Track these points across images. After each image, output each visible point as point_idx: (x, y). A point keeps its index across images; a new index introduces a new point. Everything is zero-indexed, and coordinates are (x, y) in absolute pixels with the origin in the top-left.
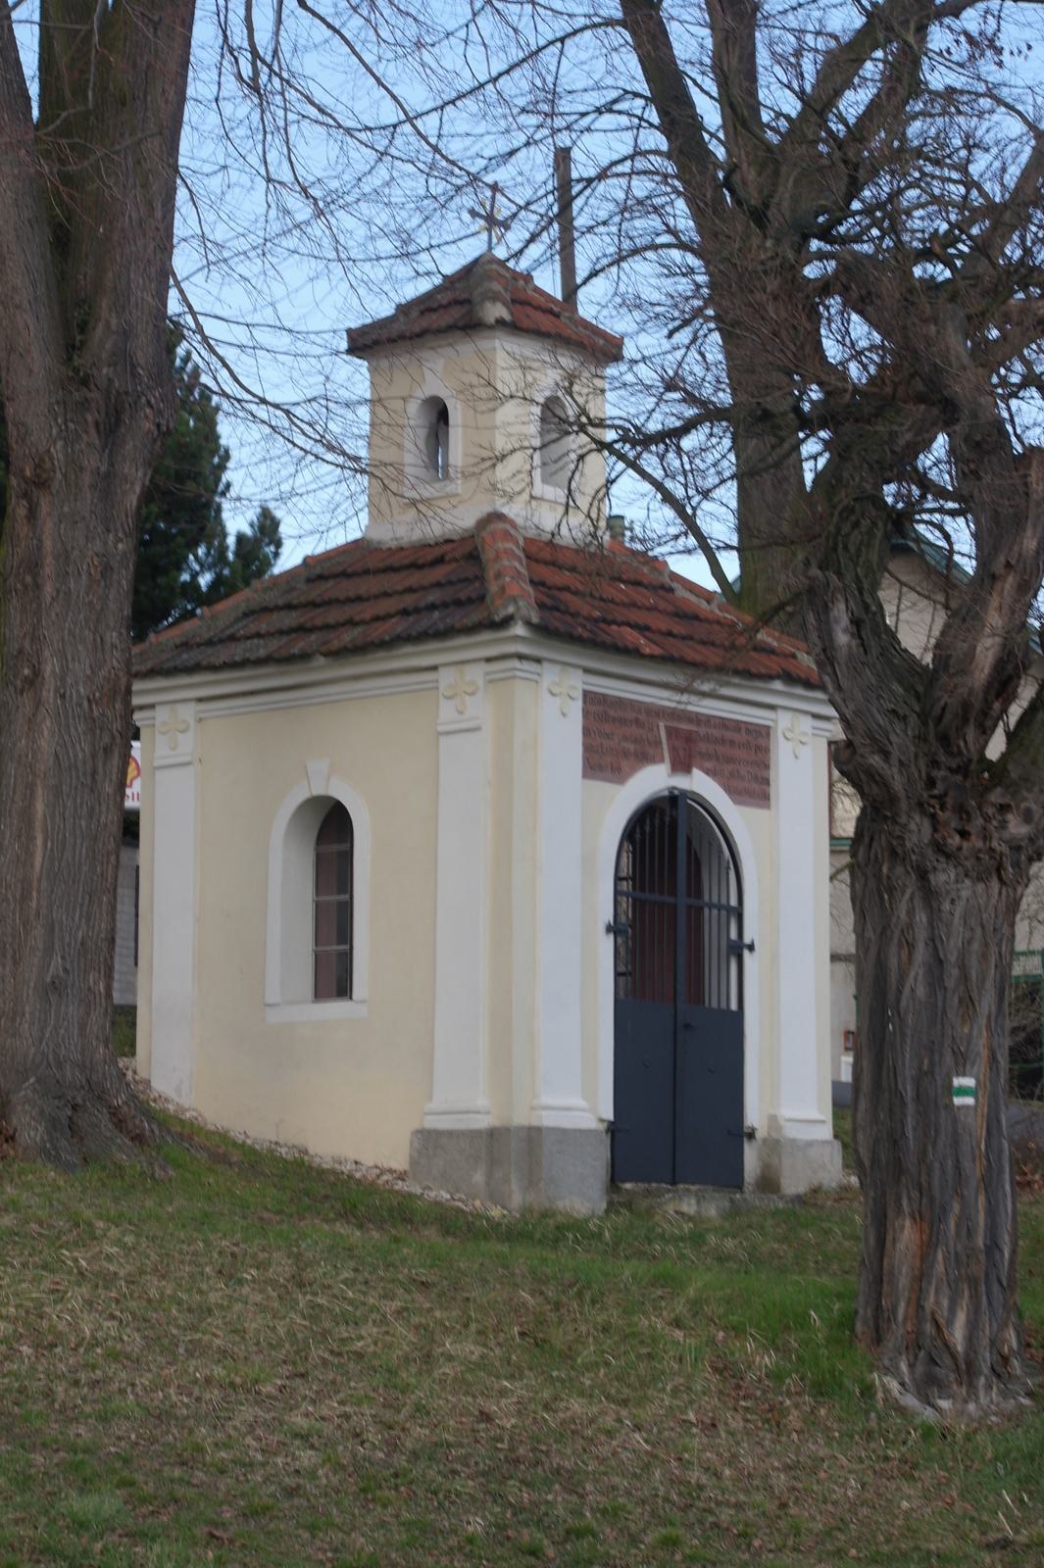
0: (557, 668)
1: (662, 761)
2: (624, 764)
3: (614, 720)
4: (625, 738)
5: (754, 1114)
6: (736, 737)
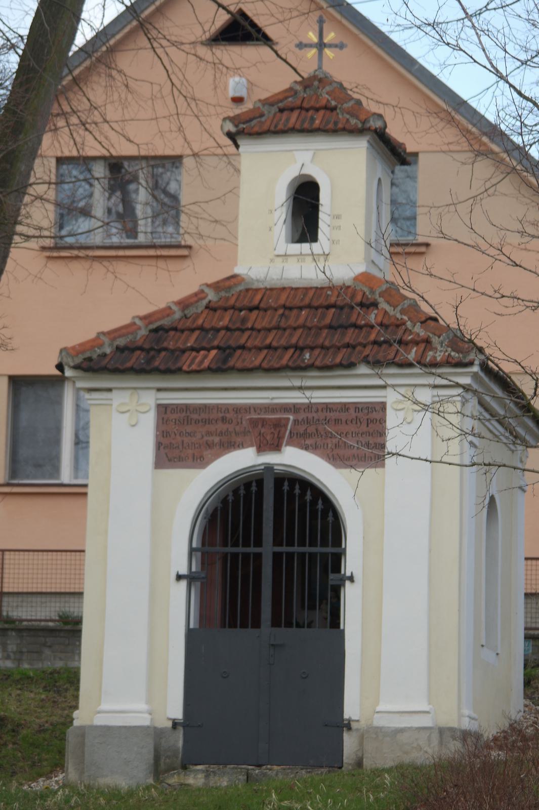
0: (129, 392)
2: (207, 453)
3: (197, 422)
4: (209, 433)
5: (351, 709)
6: (343, 416)
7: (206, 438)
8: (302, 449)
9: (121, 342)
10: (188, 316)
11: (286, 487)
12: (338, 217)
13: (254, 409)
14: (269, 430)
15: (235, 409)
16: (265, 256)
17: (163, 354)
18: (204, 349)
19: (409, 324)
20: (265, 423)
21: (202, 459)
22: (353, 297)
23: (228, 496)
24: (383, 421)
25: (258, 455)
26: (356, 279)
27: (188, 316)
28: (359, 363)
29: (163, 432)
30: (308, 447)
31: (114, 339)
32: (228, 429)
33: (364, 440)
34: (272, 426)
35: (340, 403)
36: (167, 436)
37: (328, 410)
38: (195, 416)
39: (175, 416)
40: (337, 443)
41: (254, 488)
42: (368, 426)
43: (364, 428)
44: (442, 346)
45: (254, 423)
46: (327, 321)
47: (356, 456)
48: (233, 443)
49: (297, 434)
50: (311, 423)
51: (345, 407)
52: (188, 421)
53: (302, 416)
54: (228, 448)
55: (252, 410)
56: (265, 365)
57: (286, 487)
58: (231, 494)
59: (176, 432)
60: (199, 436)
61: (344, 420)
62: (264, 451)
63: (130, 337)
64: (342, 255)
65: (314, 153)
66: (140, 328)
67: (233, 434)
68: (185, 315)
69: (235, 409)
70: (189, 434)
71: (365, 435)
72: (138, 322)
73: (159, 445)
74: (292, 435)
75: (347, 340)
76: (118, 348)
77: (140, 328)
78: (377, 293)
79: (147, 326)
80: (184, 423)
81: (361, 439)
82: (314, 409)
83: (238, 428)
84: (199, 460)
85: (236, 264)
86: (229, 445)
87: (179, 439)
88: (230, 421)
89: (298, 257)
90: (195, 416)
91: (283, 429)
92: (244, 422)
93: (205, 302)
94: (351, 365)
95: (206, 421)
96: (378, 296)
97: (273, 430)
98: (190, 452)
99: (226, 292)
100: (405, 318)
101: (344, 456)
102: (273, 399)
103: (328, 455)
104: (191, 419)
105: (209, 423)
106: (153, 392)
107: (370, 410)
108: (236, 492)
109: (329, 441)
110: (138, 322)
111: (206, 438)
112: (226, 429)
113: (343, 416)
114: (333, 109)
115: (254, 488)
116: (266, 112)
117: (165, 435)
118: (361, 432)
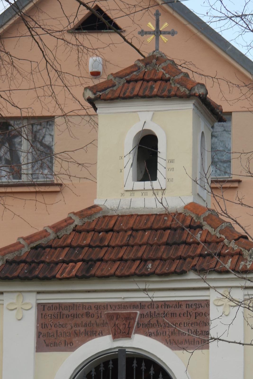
0: (16, 295)
1: (110, 334)
2: (75, 340)
3: (67, 316)
4: (77, 325)
6: (177, 311)
7: (74, 329)
8: (147, 336)
9: (10, 257)
10: (60, 237)
11: (135, 365)
12: (172, 161)
13: (110, 306)
14: (122, 322)
15: (96, 307)
16: (116, 190)
17: (42, 265)
18: (72, 261)
19: (226, 241)
20: (118, 317)
21: (71, 344)
22: (183, 221)
23: (91, 371)
24: (207, 314)
25: (114, 341)
26: (186, 207)
27: (60, 237)
28: (189, 271)
29: (42, 324)
30: (151, 334)
31: (4, 255)
32: (90, 321)
33: (192, 328)
34: (124, 319)
35: (175, 301)
36: (45, 327)
37: (166, 306)
38: (66, 312)
39: (50, 312)
40: (173, 331)
41: (111, 366)
42: (196, 318)
43: (193, 319)
44: (251, 258)
45: (110, 317)
46: (165, 239)
47: (187, 341)
48: (94, 332)
49: (143, 324)
50: (153, 316)
51: (178, 304)
52: (61, 316)
53: (146, 311)
54: (91, 336)
55: (109, 307)
56: (118, 273)
57: (135, 365)
58: (94, 370)
59: (52, 324)
60: (69, 327)
61: (178, 314)
62: (118, 337)
63: (17, 253)
64: (176, 188)
65: (154, 114)
66: (23, 247)
67: (95, 326)
68: (58, 236)
69: (96, 307)
70: (62, 326)
71: (194, 325)
72: (22, 242)
73: (39, 335)
74: (139, 325)
75: (179, 254)
76: (7, 261)
77: (23, 247)
78: (202, 218)
79: (29, 245)
80: (57, 318)
81: (191, 328)
82: (155, 305)
83: (98, 321)
84: (69, 345)
85: (96, 198)
86: (92, 333)
87: (54, 329)
88: (93, 316)
89: (143, 192)
90: (66, 312)
91: (132, 321)
92: (103, 316)
93: (72, 226)
94: (183, 273)
95: (74, 316)
96: (202, 220)
97: (124, 322)
98: (63, 339)
99: (88, 218)
100: (223, 237)
101: (178, 341)
102: (124, 298)
103: (166, 340)
104: (63, 314)
105: (76, 318)
106: (35, 294)
107: (197, 306)
108: (97, 368)
109: (167, 329)
110: (22, 242)
111: (74, 329)
112: (90, 321)
113: (177, 311)
114: (168, 80)
115: (111, 366)
116: (117, 83)
117: (43, 327)
118: (190, 323)
